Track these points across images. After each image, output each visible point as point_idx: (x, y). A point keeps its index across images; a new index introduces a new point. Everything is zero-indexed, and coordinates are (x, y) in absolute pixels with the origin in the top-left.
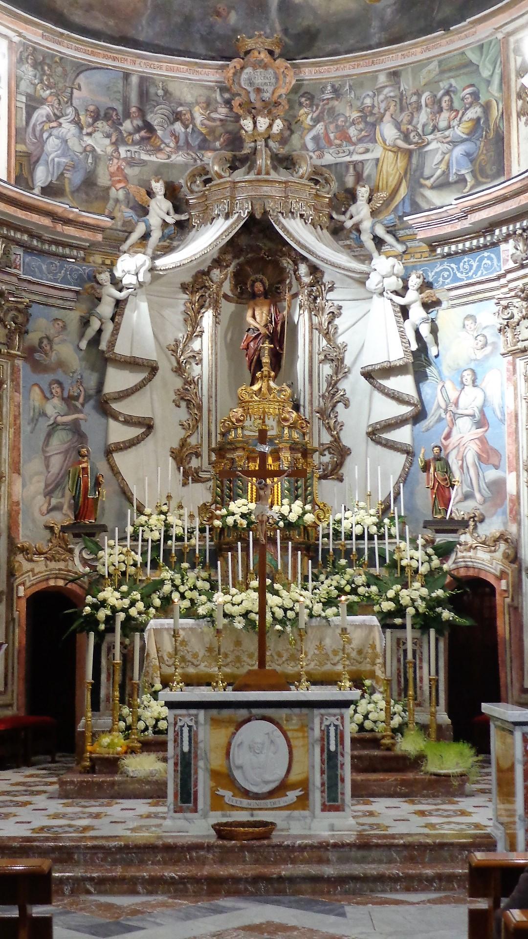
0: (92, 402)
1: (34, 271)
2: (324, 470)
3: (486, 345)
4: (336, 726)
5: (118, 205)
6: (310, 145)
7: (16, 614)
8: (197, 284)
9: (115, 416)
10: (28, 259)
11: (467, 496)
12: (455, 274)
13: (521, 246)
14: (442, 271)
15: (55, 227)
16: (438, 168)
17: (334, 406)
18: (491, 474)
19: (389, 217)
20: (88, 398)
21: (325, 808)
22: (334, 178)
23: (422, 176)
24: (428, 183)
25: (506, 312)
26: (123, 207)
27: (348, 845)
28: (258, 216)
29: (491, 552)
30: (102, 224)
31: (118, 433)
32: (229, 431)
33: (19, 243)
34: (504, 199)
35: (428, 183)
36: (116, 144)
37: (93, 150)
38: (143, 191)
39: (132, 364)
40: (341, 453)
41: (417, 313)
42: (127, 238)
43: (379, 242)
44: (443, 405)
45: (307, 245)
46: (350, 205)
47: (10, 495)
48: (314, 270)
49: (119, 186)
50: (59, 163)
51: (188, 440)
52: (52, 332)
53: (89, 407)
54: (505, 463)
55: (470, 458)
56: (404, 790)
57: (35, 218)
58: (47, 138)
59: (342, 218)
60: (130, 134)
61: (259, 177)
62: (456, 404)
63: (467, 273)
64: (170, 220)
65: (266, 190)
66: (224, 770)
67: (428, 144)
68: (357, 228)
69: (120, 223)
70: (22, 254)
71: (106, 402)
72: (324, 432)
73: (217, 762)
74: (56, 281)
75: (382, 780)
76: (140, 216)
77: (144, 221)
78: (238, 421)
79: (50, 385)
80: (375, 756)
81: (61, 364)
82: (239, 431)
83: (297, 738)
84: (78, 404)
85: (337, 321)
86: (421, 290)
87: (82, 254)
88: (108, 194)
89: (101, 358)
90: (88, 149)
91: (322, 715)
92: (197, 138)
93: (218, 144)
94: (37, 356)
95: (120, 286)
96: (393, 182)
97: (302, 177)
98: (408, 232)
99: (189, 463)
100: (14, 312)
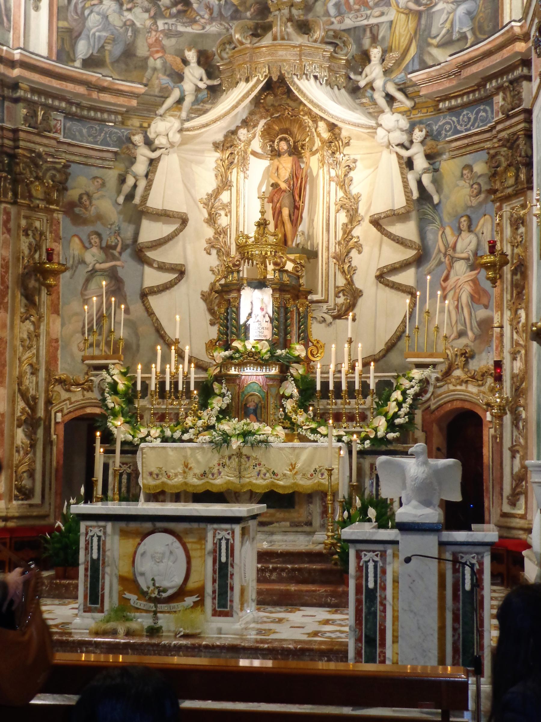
0: (129, 251)
1: (75, 135)
2: (338, 311)
3: (479, 193)
4: (227, 540)
5: (156, 73)
6: (332, 11)
7: (54, 437)
8: (227, 143)
9: (149, 263)
10: (69, 124)
11: (461, 334)
12: (455, 127)
13: (509, 99)
14: (444, 124)
15: (90, 95)
16: (443, 28)
17: (348, 252)
18: (482, 313)
19: (399, 76)
20: (125, 247)
21: (215, 613)
22: (352, 41)
23: (429, 36)
24: (435, 42)
25: (494, 161)
26: (161, 75)
27: (218, 646)
28: (275, 79)
29: (479, 386)
30: (136, 91)
31: (152, 278)
33: (57, 109)
34: (488, 54)
35: (435, 42)
36: (154, 18)
37: (133, 24)
38: (179, 60)
39: (164, 215)
40: (353, 295)
41: (420, 163)
42: (163, 103)
43: (390, 99)
44: (443, 250)
45: (320, 104)
46: (365, 66)
47: (48, 333)
48: (332, 127)
49: (157, 55)
50: (100, 37)
52: (91, 189)
53: (126, 255)
54: (493, 303)
55: (465, 298)
56: (334, 601)
57: (70, 87)
58: (89, 15)
59: (358, 78)
60: (168, 8)
61: (275, 42)
62: (454, 248)
63: (466, 125)
64: (202, 85)
65: (282, 53)
66: (131, 576)
67: (436, 4)
68: (370, 86)
69: (157, 90)
70: (62, 119)
71: (141, 250)
73: (125, 569)
74: (96, 143)
75: (314, 591)
76: (175, 83)
77: (178, 87)
78: (234, 265)
79: (89, 236)
80: (315, 570)
81: (99, 217)
82: (235, 275)
83: (196, 550)
84: (116, 253)
85: (352, 174)
86: (422, 142)
87: (120, 118)
88: (146, 63)
89: (137, 212)
90: (128, 23)
91: (216, 530)
92: (229, 9)
93: (248, 14)
94: (77, 210)
95: (153, 147)
96: (404, 42)
97: (315, 41)
98: (416, 88)
100: (54, 172)
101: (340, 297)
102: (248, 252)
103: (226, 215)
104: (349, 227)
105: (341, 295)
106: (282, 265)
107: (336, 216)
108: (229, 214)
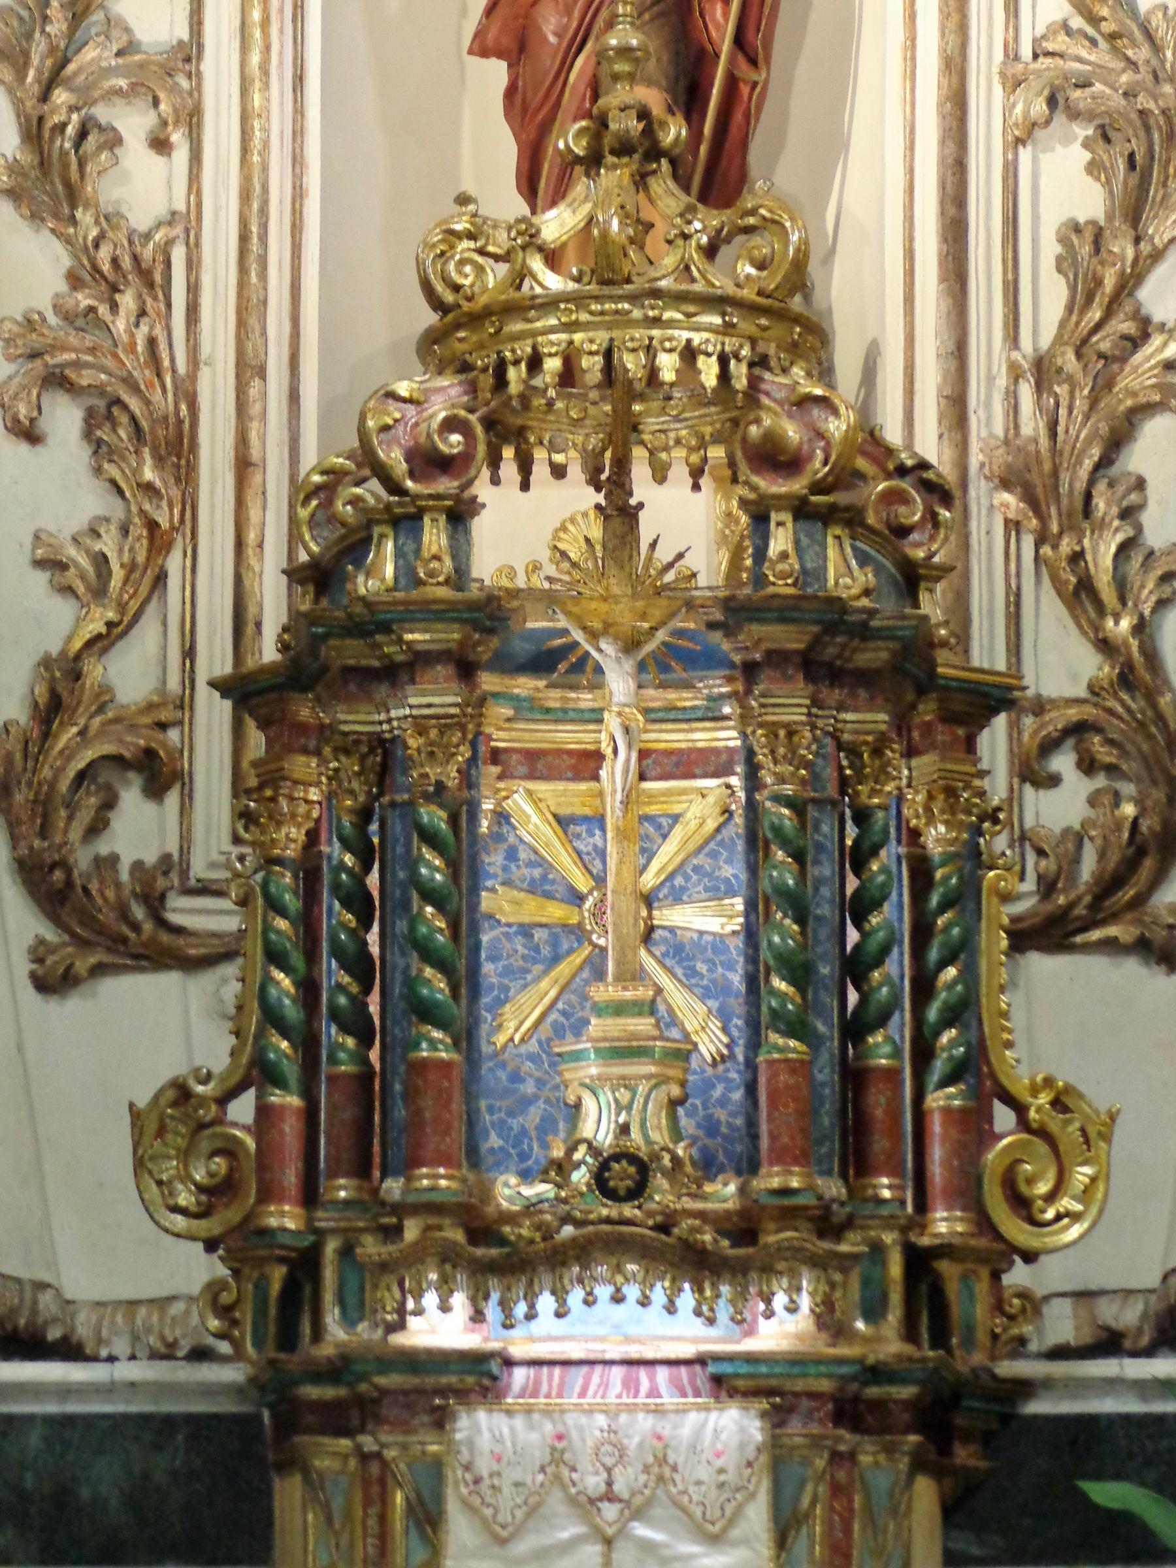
2: (1047, 887)
17: (1117, 440)
32: (355, 547)
51: (95, 671)
72: (1048, 617)
78: (429, 462)
82: (434, 536)
99: (97, 828)
101: (1054, 781)
102: (535, 363)
103: (160, 144)
104: (1123, 248)
105: (1063, 762)
106: (818, 468)
107: (1011, 171)
108: (177, 137)
